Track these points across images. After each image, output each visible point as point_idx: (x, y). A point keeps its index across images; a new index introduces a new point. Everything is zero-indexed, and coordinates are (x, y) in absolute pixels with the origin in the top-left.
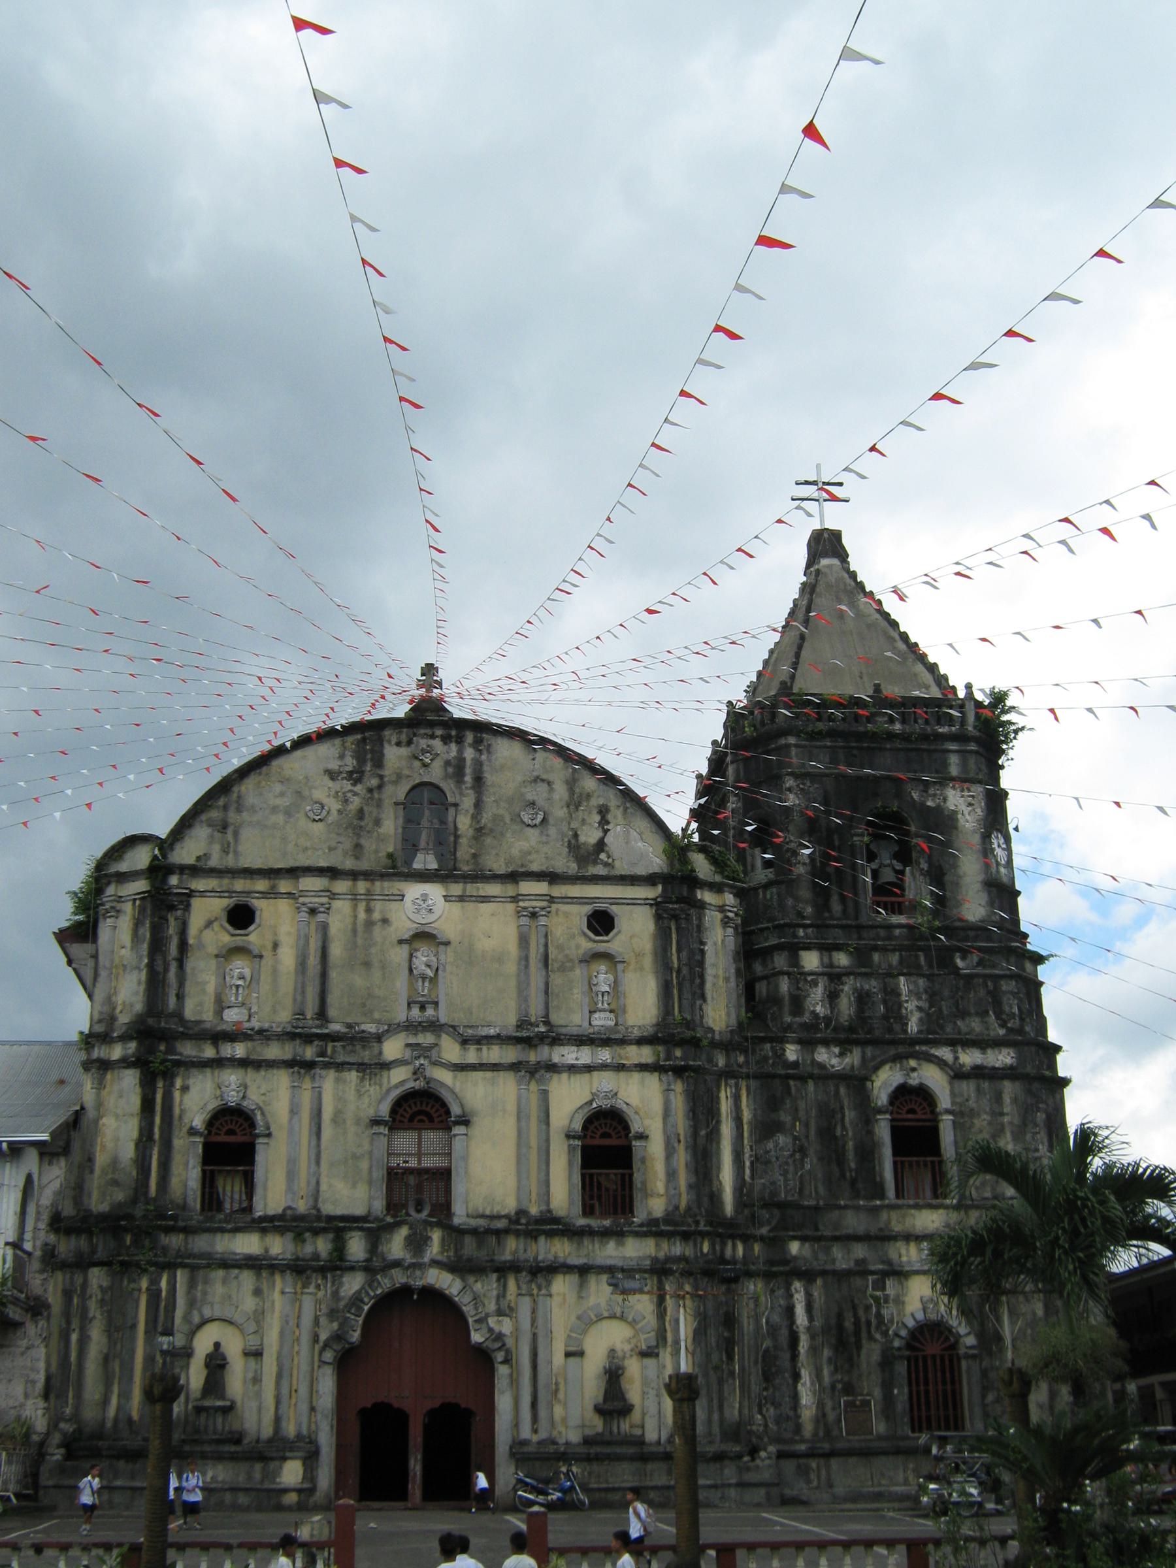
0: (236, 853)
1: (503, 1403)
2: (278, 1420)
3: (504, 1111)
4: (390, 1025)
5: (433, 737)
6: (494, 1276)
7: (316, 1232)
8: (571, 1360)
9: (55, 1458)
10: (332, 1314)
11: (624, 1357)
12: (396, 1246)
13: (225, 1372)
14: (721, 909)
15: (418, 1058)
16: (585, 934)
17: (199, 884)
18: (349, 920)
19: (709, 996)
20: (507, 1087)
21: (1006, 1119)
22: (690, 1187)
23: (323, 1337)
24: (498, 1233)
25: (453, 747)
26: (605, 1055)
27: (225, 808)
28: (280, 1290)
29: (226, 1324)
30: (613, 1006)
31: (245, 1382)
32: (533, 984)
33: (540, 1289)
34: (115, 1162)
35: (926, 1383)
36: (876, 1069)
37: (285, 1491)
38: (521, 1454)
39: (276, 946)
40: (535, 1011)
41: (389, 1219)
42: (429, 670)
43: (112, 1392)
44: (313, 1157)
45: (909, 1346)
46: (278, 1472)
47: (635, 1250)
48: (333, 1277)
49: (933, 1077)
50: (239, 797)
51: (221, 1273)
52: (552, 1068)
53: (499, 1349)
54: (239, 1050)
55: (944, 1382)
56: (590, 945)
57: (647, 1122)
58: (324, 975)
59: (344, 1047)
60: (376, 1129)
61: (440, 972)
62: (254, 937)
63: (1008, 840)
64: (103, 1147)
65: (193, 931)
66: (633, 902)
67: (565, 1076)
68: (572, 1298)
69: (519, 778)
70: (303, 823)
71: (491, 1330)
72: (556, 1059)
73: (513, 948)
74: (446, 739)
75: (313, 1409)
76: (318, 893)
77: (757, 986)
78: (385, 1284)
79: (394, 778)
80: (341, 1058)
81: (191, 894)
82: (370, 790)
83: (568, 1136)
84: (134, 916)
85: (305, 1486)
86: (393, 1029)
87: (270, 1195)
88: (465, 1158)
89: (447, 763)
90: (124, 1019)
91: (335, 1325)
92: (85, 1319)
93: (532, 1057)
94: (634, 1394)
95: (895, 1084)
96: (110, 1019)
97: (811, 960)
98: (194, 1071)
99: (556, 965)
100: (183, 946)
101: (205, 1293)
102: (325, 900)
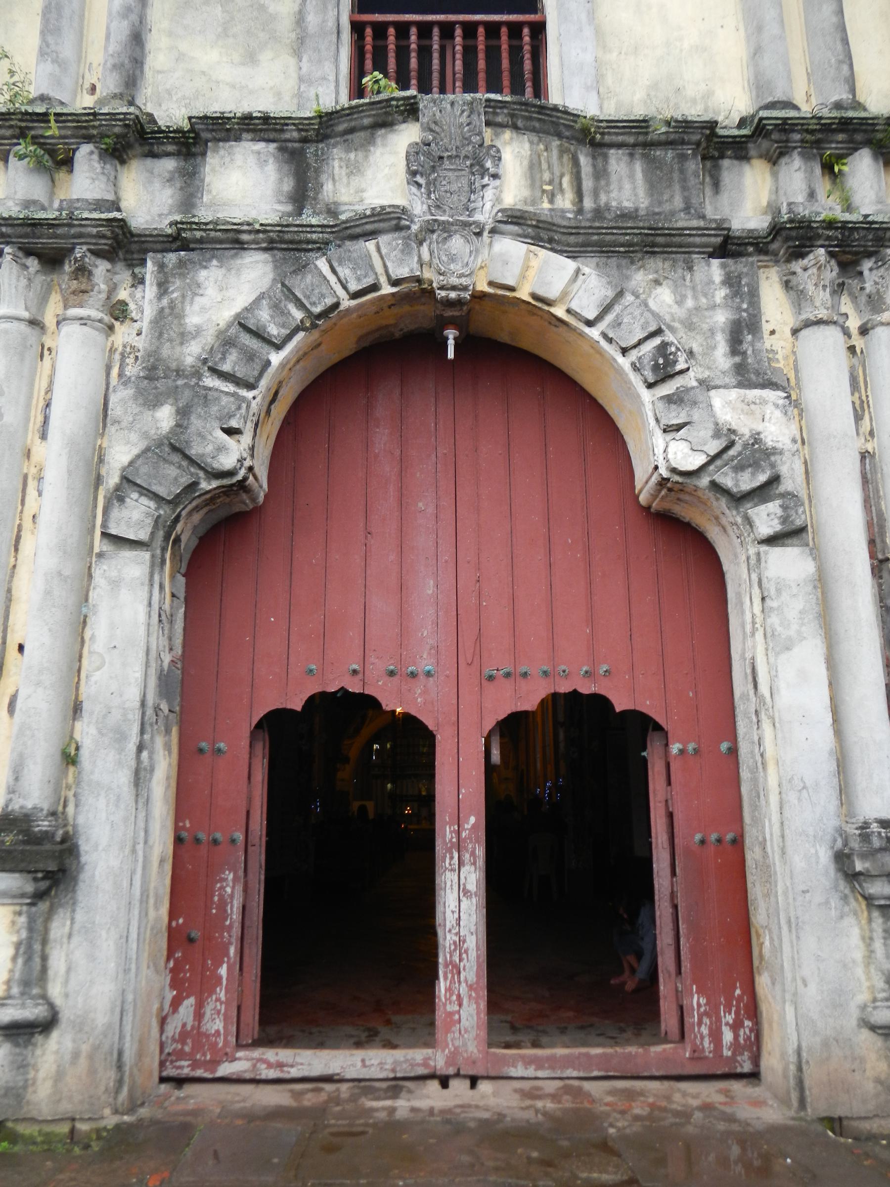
6: (716, 269)
48: (161, 266)
53: (762, 493)
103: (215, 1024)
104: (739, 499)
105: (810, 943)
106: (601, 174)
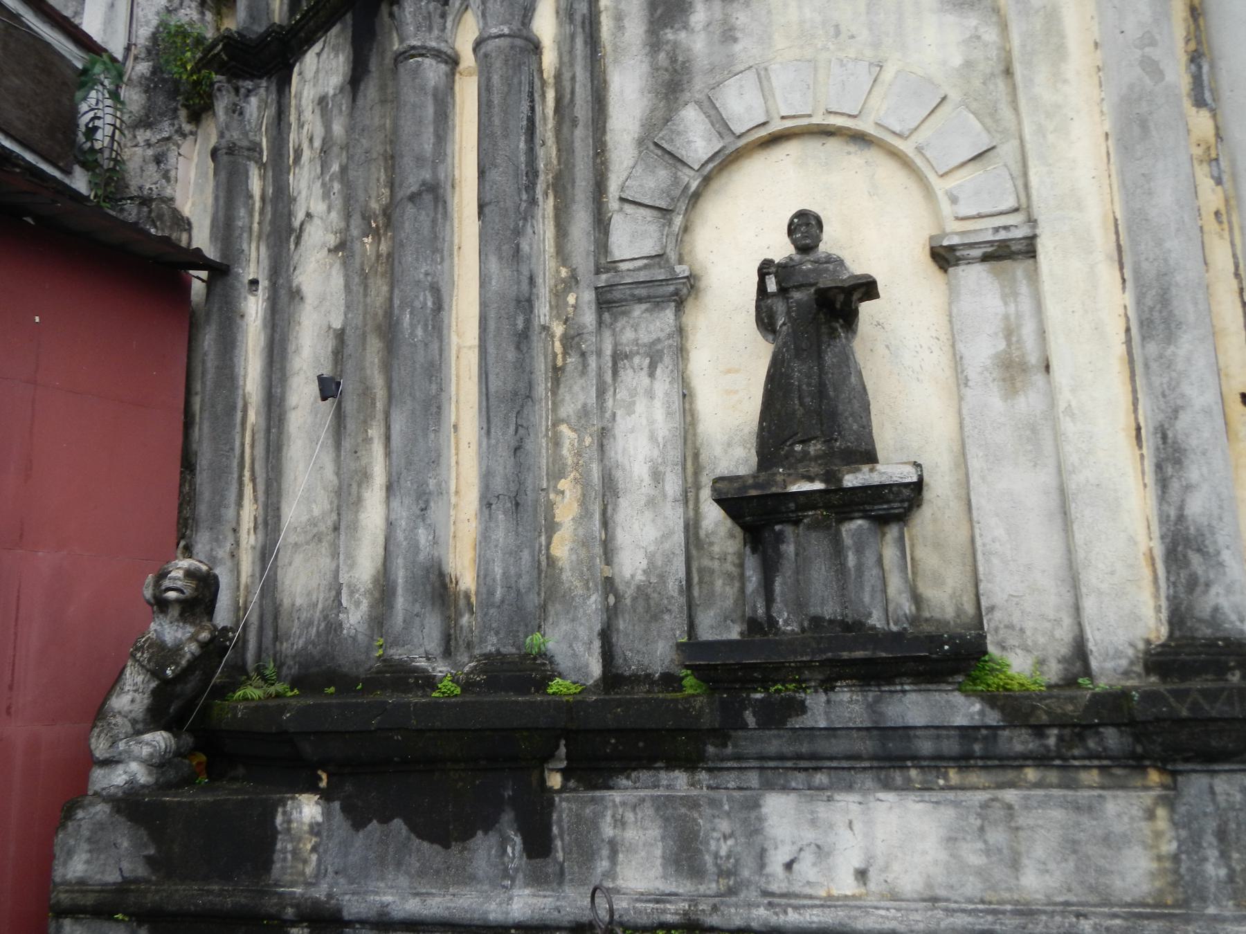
9: (117, 778)
13: (860, 346)
29: (833, 144)
43: (365, 476)
101: (728, 35)
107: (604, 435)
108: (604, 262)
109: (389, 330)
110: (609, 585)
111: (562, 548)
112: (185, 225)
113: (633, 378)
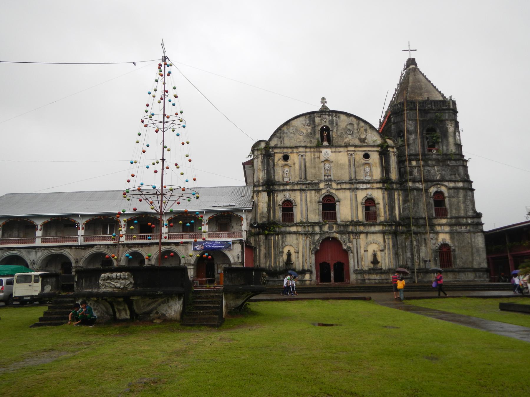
0: (284, 143)
1: (351, 261)
2: (303, 266)
3: (347, 199)
4: (321, 181)
5: (326, 115)
6: (348, 235)
7: (308, 226)
8: (366, 252)
10: (313, 243)
11: (376, 252)
12: (326, 229)
14: (394, 152)
15: (327, 188)
16: (363, 159)
17: (276, 151)
18: (310, 158)
19: (392, 172)
20: (348, 194)
21: (461, 199)
22: (389, 215)
23: (312, 248)
24: (348, 225)
25: (331, 117)
26: (369, 186)
27: (280, 133)
28: (301, 238)
30: (370, 175)
31: (295, 258)
32: (352, 170)
33: (358, 237)
34: (263, 213)
35: (443, 257)
36: (431, 187)
37: (306, 281)
38: (356, 272)
39: (294, 164)
40: (353, 177)
41: (324, 223)
42: (323, 99)
44: (306, 210)
45: (439, 249)
46: (304, 276)
47: (378, 228)
49: (443, 189)
50: (283, 131)
51: (288, 236)
52: (357, 189)
53: (350, 250)
54: (288, 187)
55: (448, 257)
56: (364, 161)
57: (379, 201)
58: (305, 170)
59: (311, 186)
60: (319, 203)
61: (331, 168)
62: (289, 162)
63: (459, 133)
64: (260, 209)
65: (276, 161)
66: (374, 151)
67: (360, 191)
68: (365, 239)
69: (346, 123)
70: (298, 136)
71: (348, 246)
72: (358, 187)
73: (347, 163)
74: (329, 115)
75: (310, 263)
76: (303, 152)
77: (401, 169)
78: (324, 237)
79: (318, 125)
80: (310, 188)
81: (275, 153)
82: (312, 128)
83: (362, 204)
84: (262, 158)
85: (310, 279)
86: (321, 181)
87: (297, 218)
88: (339, 209)
89: (330, 121)
90: (261, 181)
91: (314, 246)
92: (260, 246)
93: (353, 187)
94: (379, 259)
95: (435, 191)
96: (259, 181)
97: (414, 163)
98: (279, 192)
99: (357, 166)
100: (274, 165)
101: (285, 240)
102: (305, 153)
103: (319, 281)
104: (349, 250)
105: (352, 276)
106: (340, 227)
107: (279, 259)
108: (279, 251)
109: (269, 254)
110: (279, 267)
111: (277, 265)
112: (251, 244)
113: (281, 257)
